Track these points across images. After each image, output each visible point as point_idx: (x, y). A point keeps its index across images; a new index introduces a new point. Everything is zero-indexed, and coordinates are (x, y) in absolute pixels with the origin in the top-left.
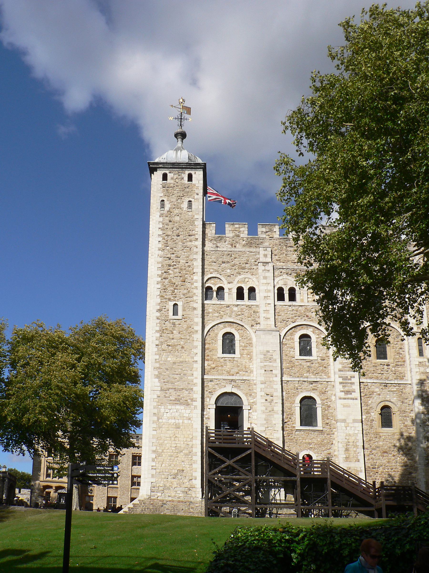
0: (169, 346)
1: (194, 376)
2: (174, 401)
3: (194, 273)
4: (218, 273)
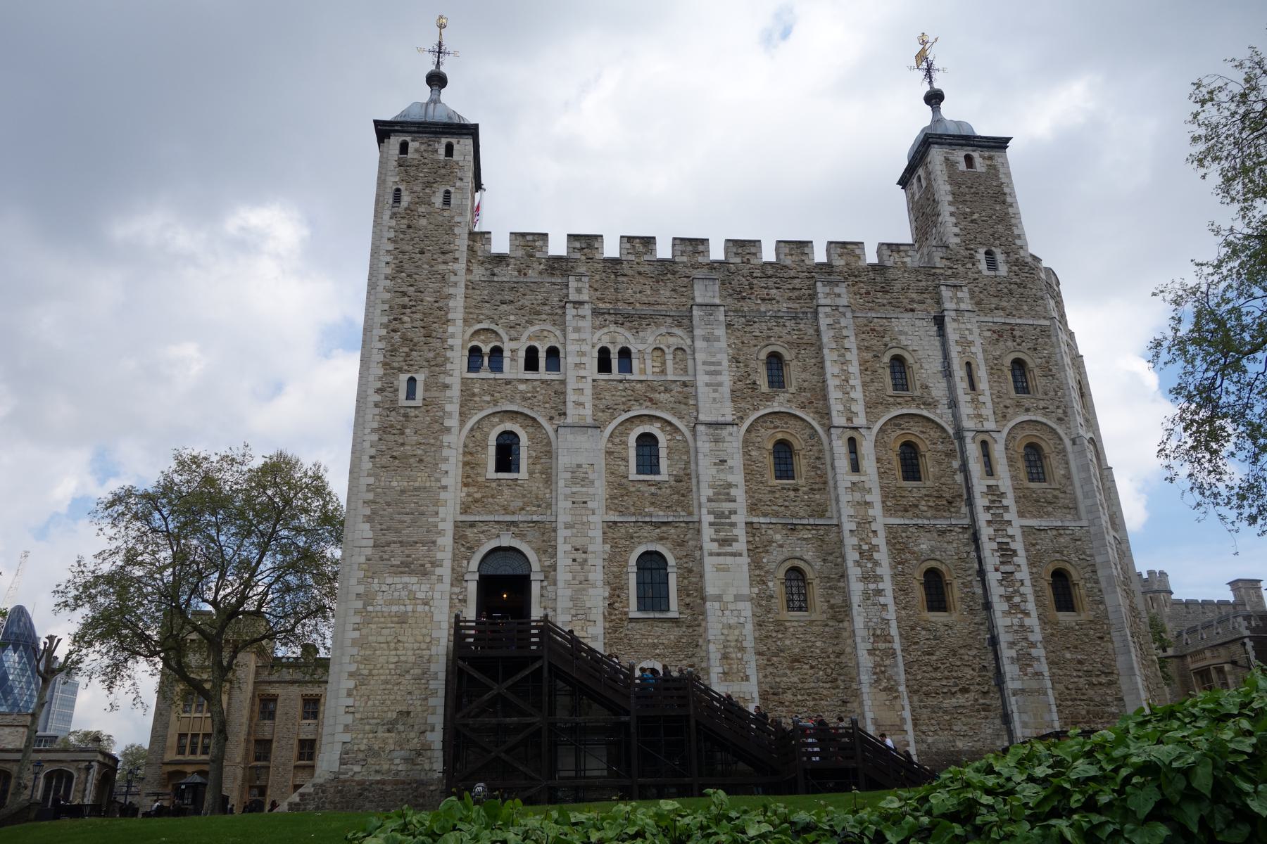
0: (395, 458)
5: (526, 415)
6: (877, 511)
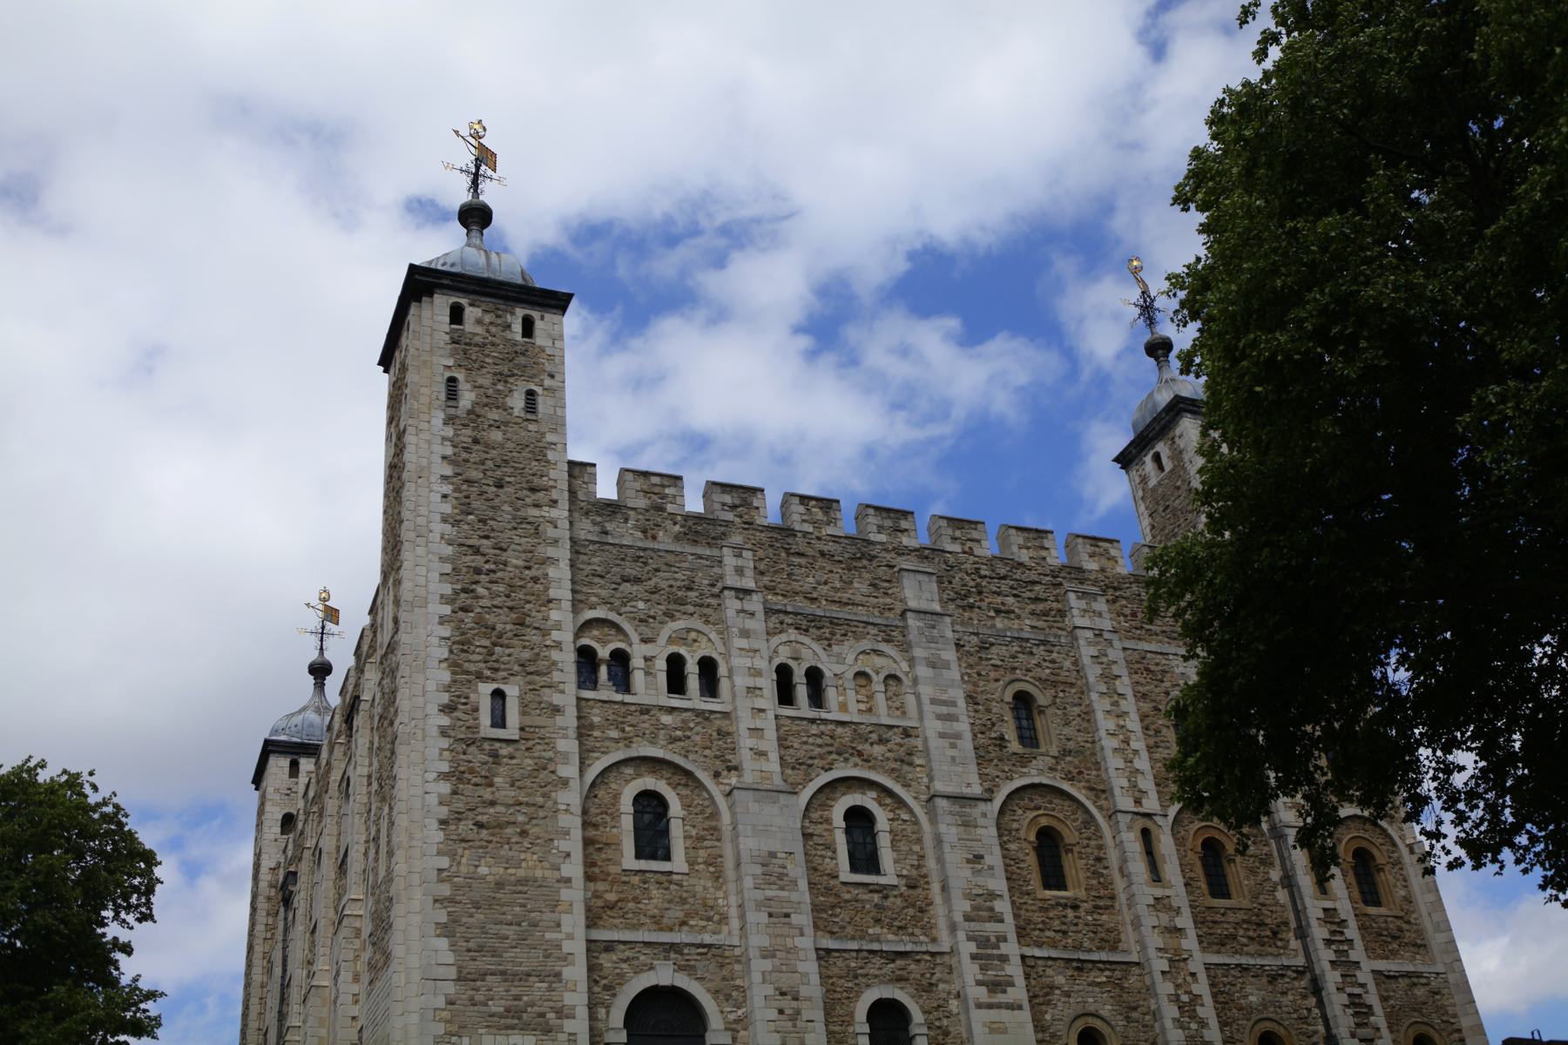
0: (480, 825)
1: (564, 929)
2: (502, 1016)
3: (550, 601)
4: (611, 610)
6: (1190, 942)
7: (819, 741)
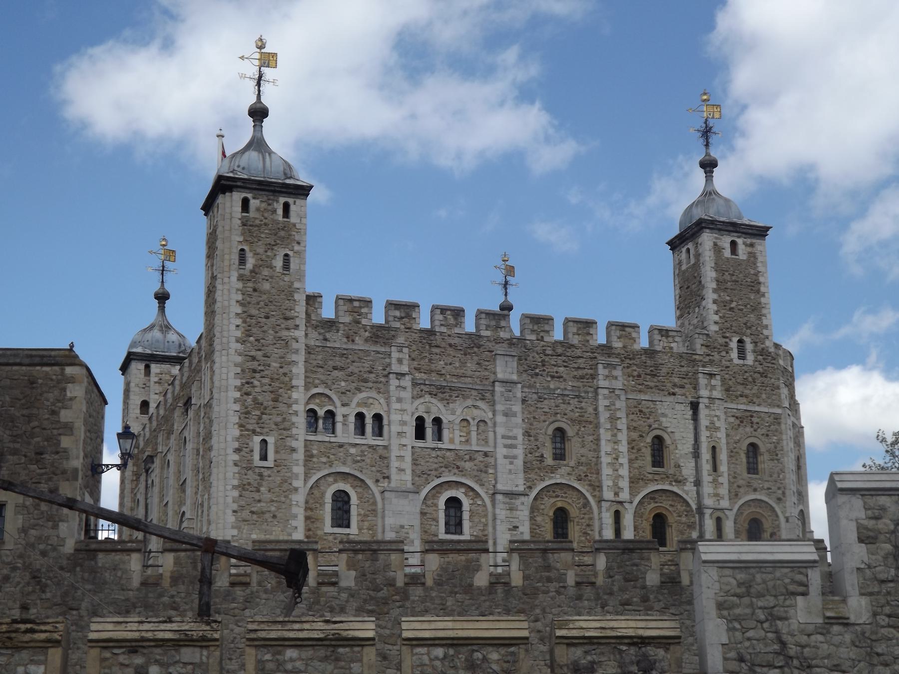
0: (252, 512)
3: (292, 387)
5: (356, 477)
7: (436, 460)
